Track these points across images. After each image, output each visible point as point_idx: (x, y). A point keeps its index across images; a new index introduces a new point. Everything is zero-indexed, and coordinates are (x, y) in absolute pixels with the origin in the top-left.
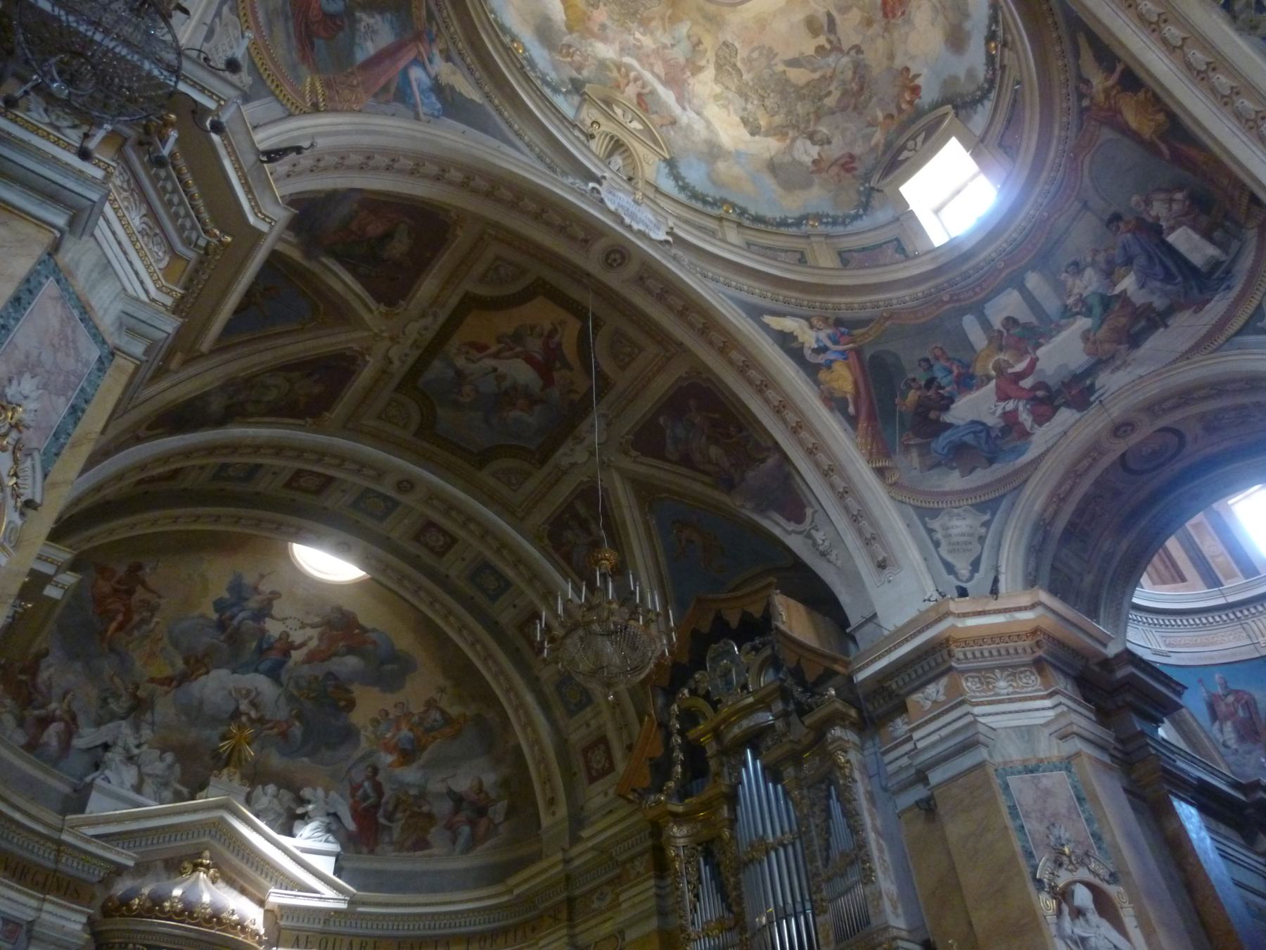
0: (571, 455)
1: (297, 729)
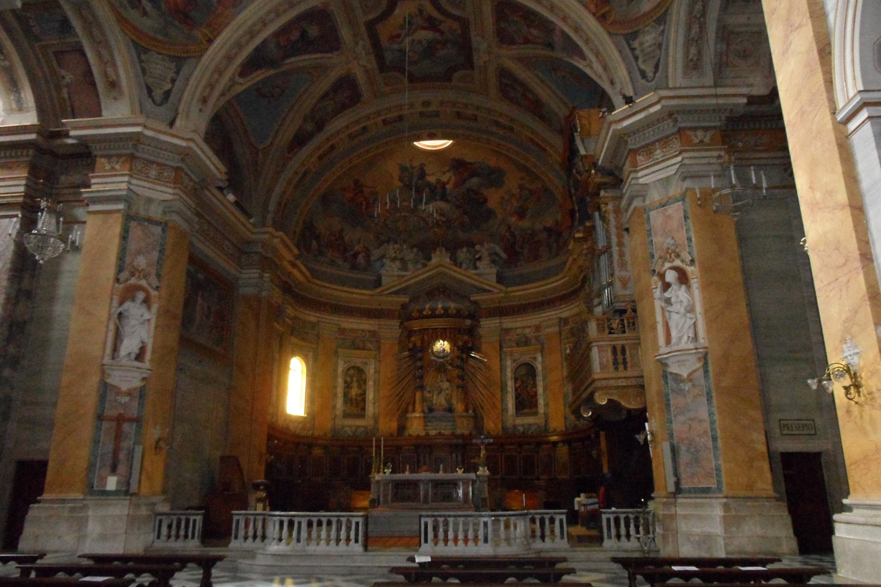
0: (480, 59)
1: (466, 219)
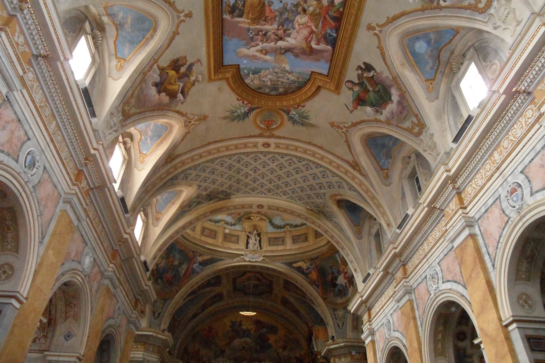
1: (258, 347)
